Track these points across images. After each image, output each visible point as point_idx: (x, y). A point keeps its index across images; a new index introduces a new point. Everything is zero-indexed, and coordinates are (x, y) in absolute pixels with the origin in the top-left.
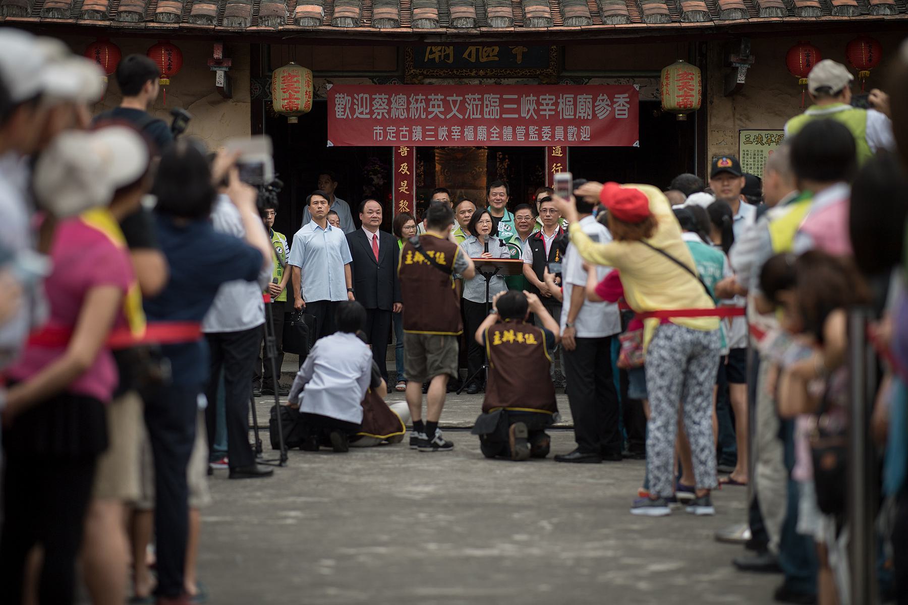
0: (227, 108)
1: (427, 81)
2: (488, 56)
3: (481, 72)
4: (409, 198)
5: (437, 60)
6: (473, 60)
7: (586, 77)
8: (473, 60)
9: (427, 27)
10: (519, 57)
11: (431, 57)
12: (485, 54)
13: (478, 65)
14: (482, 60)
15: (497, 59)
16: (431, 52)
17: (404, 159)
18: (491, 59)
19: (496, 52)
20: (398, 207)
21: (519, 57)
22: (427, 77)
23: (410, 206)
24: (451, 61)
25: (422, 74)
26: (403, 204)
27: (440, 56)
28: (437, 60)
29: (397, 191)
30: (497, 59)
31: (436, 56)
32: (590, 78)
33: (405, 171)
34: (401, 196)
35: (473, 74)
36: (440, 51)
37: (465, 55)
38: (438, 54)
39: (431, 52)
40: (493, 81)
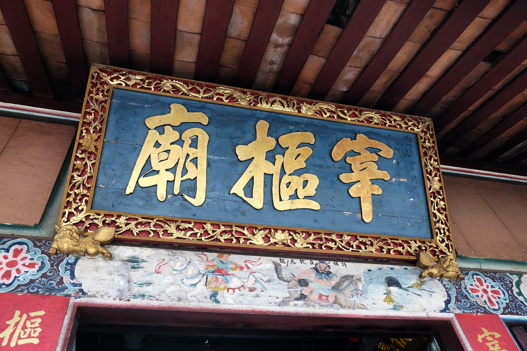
2: (294, 196)
6: (257, 201)
8: (257, 201)
10: (367, 208)
11: (145, 182)
12: (286, 193)
15: (315, 205)
16: (148, 170)
21: (367, 208)
24: (199, 200)
27: (170, 183)
28: (161, 193)
30: (315, 205)
31: (160, 182)
35: (258, 240)
36: (173, 170)
37: (238, 189)
39: (148, 170)
40: (308, 264)
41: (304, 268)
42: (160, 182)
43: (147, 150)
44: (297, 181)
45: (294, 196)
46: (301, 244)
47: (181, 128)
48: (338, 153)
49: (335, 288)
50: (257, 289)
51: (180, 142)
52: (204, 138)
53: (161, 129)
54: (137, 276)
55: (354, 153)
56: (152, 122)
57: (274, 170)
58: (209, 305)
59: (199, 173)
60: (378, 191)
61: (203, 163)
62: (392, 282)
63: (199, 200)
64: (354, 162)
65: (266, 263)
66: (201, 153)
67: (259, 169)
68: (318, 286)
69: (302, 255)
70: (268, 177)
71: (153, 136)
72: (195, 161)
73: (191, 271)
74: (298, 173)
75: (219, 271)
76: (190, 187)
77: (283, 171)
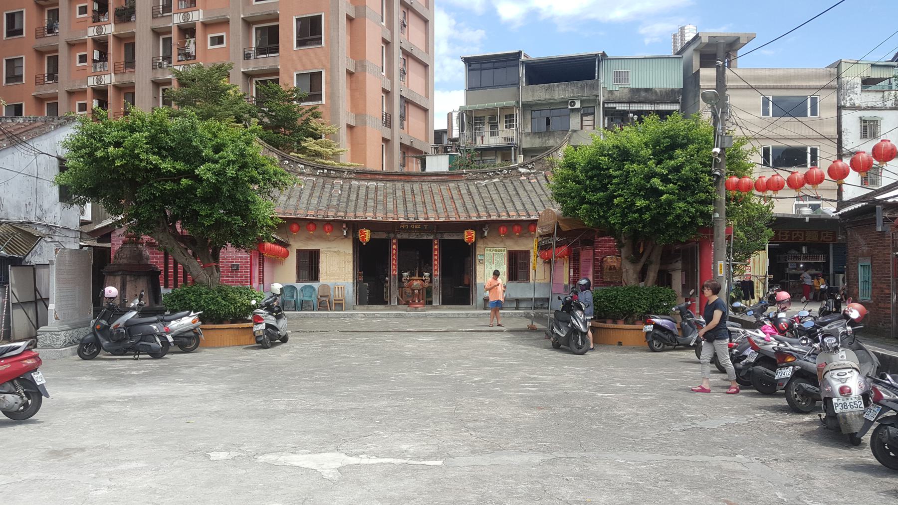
0: (346, 240)
9: (402, 220)
13: (415, 229)
50: (413, 237)
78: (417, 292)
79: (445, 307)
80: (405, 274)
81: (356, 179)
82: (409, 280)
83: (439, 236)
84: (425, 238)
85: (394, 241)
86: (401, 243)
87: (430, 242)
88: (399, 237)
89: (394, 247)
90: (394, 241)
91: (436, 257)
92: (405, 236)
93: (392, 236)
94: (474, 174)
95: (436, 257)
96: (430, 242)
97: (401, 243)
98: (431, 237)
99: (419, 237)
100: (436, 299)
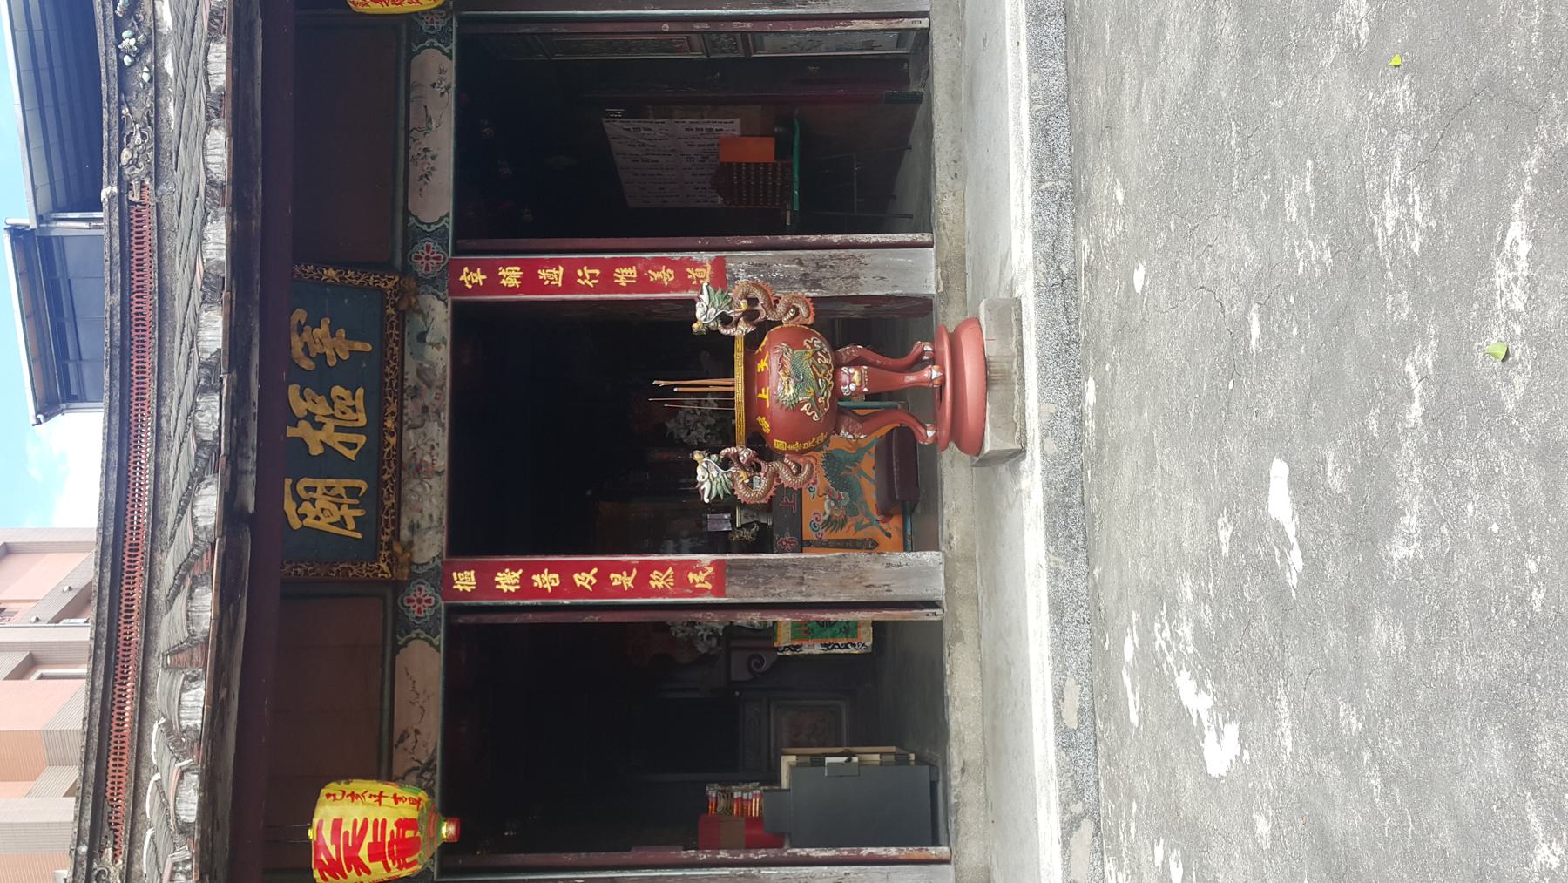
1: (405, 534)
2: (354, 409)
3: (389, 424)
4: (645, 570)
5: (358, 513)
6: (361, 440)
7: (406, 221)
8: (361, 440)
10: (358, 346)
11: (351, 525)
12: (350, 415)
13: (375, 429)
14: (363, 421)
15: (360, 392)
16: (342, 523)
17: (567, 581)
18: (360, 404)
19: (346, 393)
20: (663, 592)
21: (358, 346)
22: (396, 535)
23: (662, 567)
24: (363, 485)
25: (389, 544)
26: (657, 580)
27: (351, 506)
28: (358, 513)
29: (630, 593)
30: (360, 392)
31: (350, 514)
32: (407, 213)
33: (590, 577)
34: (641, 585)
35: (393, 441)
36: (339, 506)
37: (351, 454)
38: (345, 510)
39: (342, 523)
40: (408, 403)
41: (410, 407)
42: (350, 514)
43: (323, 525)
44: (338, 404)
45: (354, 409)
46: (394, 408)
47: (299, 501)
48: (307, 364)
49: (429, 386)
50: (432, 443)
51: (313, 501)
52: (307, 482)
53: (302, 517)
54: (425, 524)
55: (306, 349)
56: (296, 523)
57: (330, 425)
58: (445, 477)
59: (340, 485)
60: (342, 332)
61: (330, 482)
62: (422, 337)
63: (363, 485)
64: (316, 349)
65: (410, 435)
66: (320, 484)
67: (335, 440)
68: (429, 397)
69: (401, 407)
70: (338, 429)
71: (309, 522)
72: (329, 488)
73: (419, 489)
74: (331, 404)
75: (418, 468)
76: (352, 492)
77: (332, 416)
78: (852, 380)
79: (945, 204)
80: (709, 477)
81: (133, 843)
82: (756, 440)
83: (431, 257)
84: (440, 357)
85: (465, 581)
86: (475, 535)
87: (476, 322)
88: (431, 547)
89: (507, 581)
90: (465, 581)
91: (587, 276)
92: (429, 502)
93: (424, 602)
94: (124, 138)
95: (587, 276)
96: (476, 322)
97: (475, 535)
98: (439, 316)
99: (440, 398)
100: (885, 268)
